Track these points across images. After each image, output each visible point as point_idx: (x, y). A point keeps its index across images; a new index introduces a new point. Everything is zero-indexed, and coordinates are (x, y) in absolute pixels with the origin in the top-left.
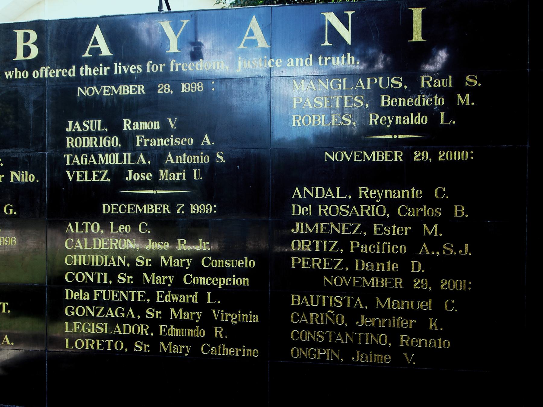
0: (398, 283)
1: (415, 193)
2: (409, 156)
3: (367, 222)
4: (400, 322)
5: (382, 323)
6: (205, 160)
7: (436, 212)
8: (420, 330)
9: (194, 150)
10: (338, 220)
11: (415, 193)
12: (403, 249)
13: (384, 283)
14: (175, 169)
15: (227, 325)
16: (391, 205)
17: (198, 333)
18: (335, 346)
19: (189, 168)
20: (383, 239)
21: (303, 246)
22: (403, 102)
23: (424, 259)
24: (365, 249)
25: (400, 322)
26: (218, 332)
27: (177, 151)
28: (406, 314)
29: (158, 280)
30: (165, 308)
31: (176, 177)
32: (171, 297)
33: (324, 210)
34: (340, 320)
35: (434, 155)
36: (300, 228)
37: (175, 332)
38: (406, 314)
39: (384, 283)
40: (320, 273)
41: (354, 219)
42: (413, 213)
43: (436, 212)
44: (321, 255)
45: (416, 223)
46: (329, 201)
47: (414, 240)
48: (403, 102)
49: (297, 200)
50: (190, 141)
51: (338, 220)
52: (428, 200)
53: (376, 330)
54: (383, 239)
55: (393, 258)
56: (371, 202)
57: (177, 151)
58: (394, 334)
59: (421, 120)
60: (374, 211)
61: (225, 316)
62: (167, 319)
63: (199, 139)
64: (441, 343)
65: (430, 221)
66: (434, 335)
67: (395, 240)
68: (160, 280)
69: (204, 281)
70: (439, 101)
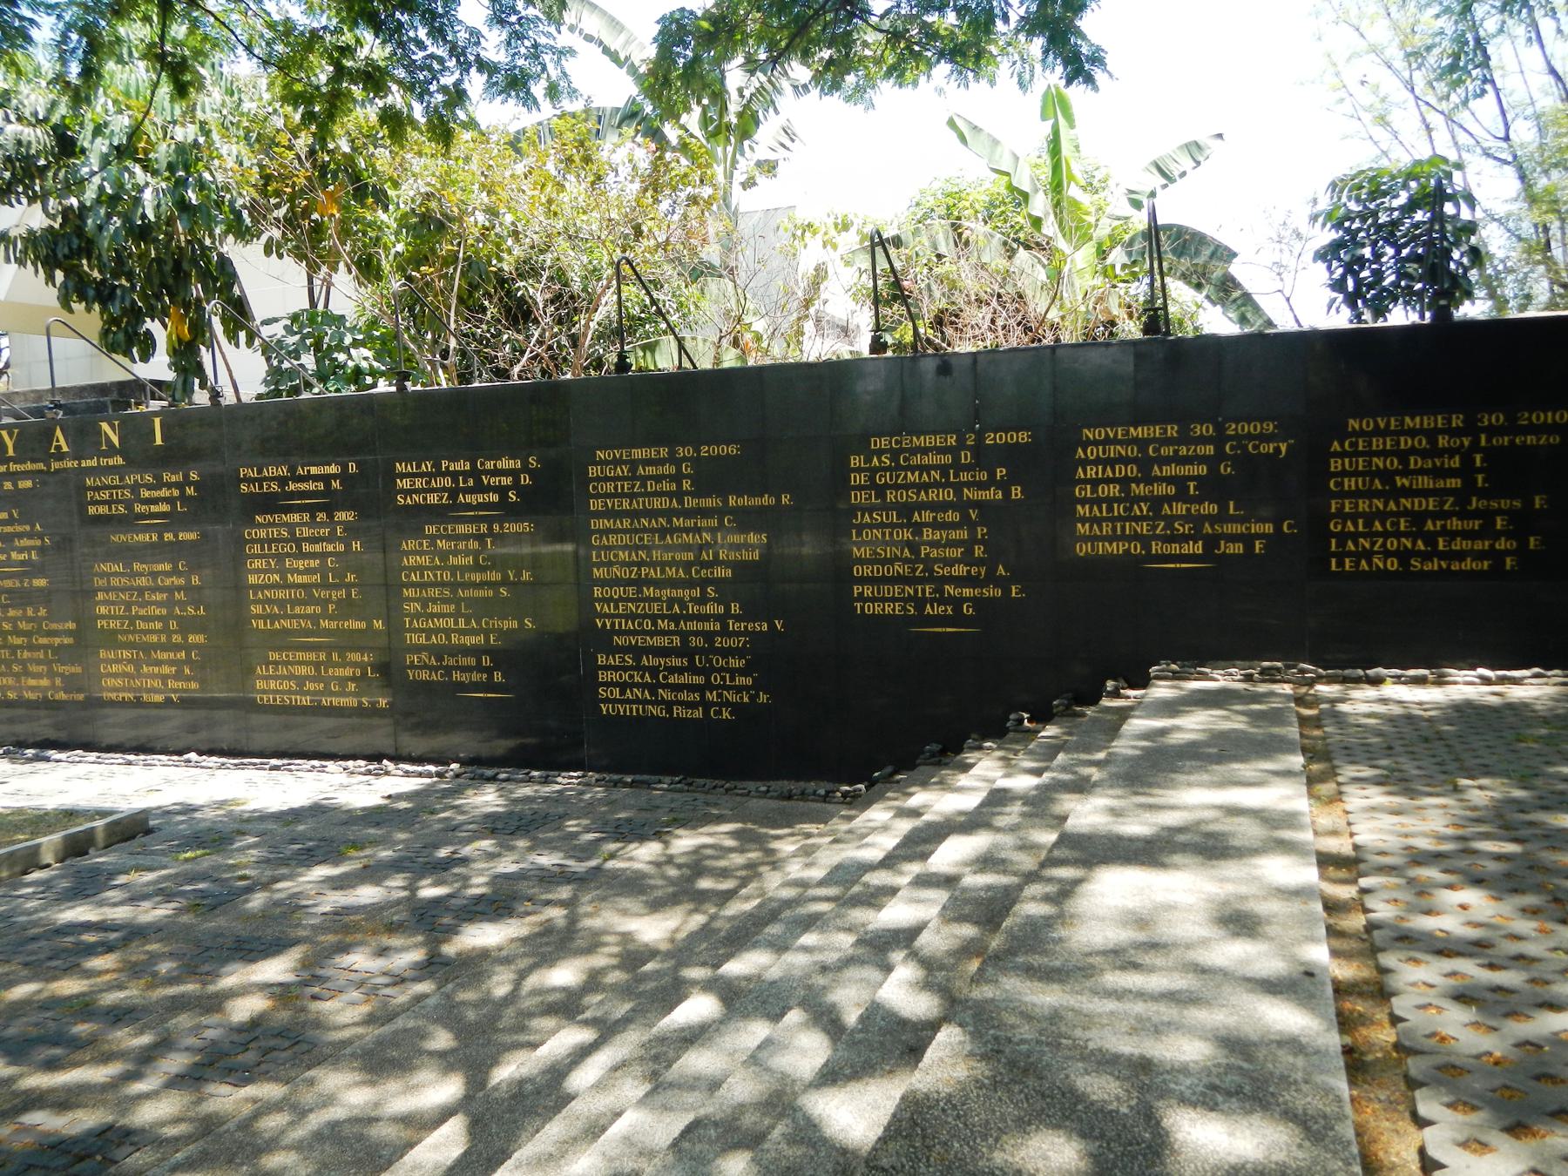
0: (163, 639)
1: (168, 567)
2: (161, 537)
3: (141, 591)
4: (166, 670)
5: (156, 670)
6: (38, 543)
7: (182, 581)
8: (178, 676)
9: (30, 536)
10: (123, 590)
11: (168, 567)
12: (164, 611)
13: (155, 638)
14: (21, 550)
15: (62, 675)
16: (154, 575)
17: (45, 682)
18: (129, 690)
19: (28, 549)
20: (152, 603)
21: (103, 610)
22: (156, 494)
23: (180, 619)
24: (142, 612)
25: (166, 670)
26: (58, 681)
27: (20, 536)
28: (171, 663)
29: (18, 641)
30: (23, 663)
31: (21, 557)
32: (26, 654)
33: (115, 582)
34: (130, 669)
35: (176, 536)
36: (100, 596)
37: (32, 682)
38: (171, 663)
39: (155, 638)
40: (114, 632)
41: (131, 589)
42: (168, 582)
43: (182, 581)
44: (115, 617)
45: (170, 590)
46: (116, 574)
47: (170, 604)
48: (156, 494)
49: (96, 575)
50: (28, 528)
51: (123, 590)
52: (175, 572)
53: (153, 676)
54: (152, 603)
55: (159, 618)
56: (141, 574)
57: (20, 536)
58: (164, 678)
59: (165, 508)
60: (142, 582)
61: (61, 669)
62: (27, 673)
63: (33, 526)
64: (194, 685)
65: (179, 589)
66: (188, 679)
67: (159, 604)
68: (18, 641)
69: (43, 641)
70: (176, 493)
